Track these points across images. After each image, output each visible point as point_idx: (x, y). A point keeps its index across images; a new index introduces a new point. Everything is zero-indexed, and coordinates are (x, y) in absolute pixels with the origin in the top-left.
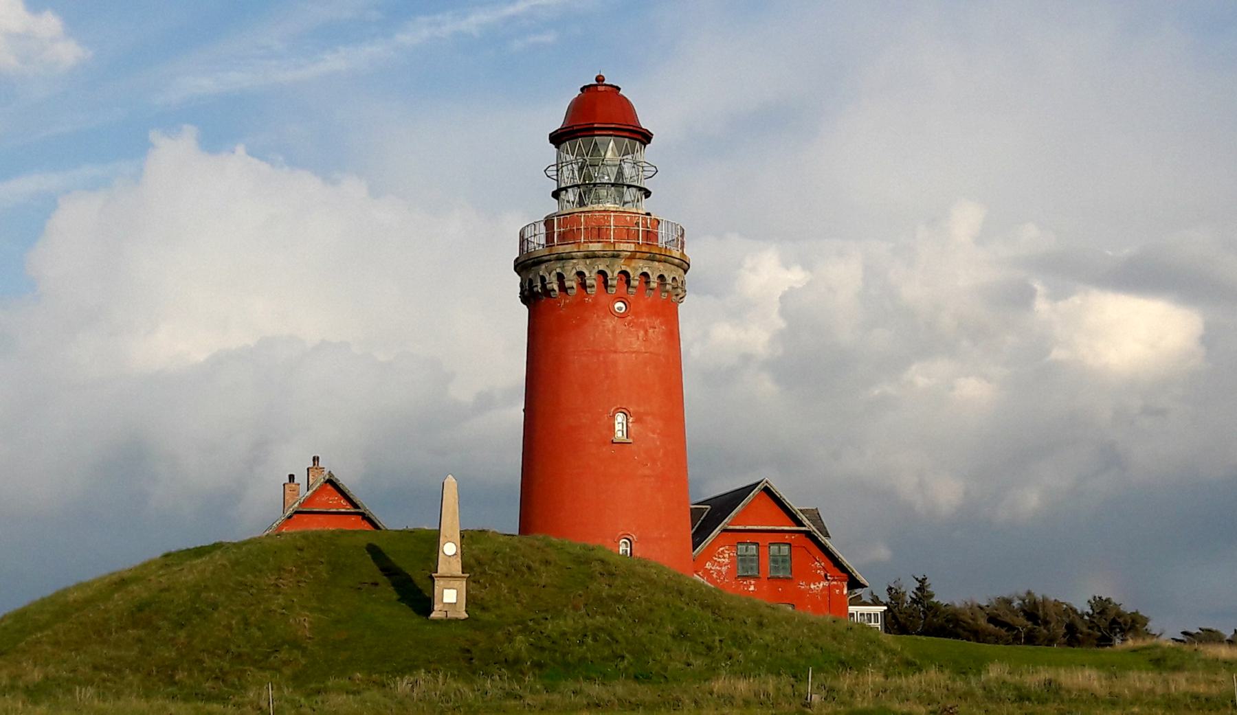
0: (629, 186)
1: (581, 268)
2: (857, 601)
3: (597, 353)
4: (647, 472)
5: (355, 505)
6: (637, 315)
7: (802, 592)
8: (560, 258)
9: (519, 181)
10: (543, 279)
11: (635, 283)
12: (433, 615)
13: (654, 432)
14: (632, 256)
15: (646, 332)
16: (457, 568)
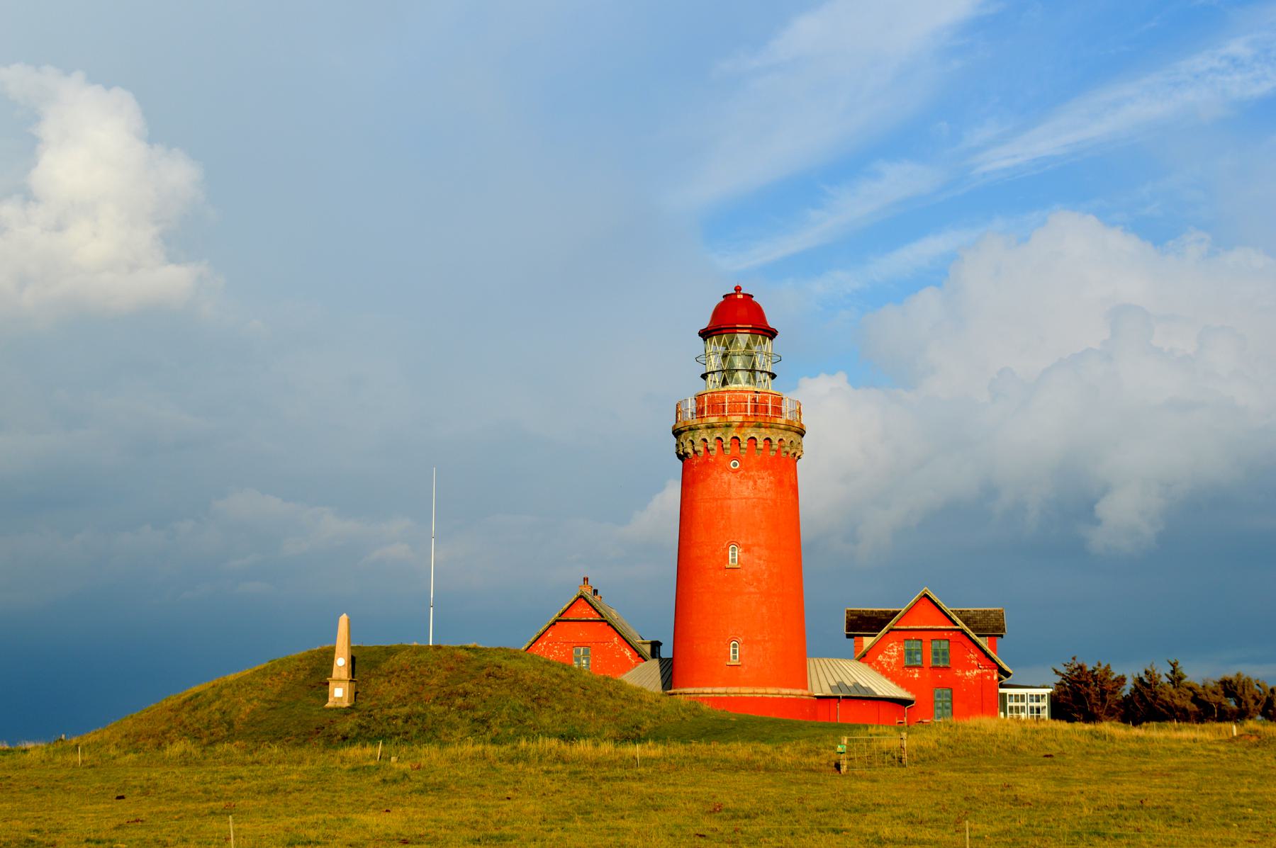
1: (704, 436)
2: (1002, 686)
3: (717, 500)
4: (753, 590)
5: (601, 615)
6: (747, 470)
7: (962, 678)
11: (744, 445)
12: (328, 705)
13: (760, 558)
14: (741, 426)
15: (755, 482)
16: (345, 674)
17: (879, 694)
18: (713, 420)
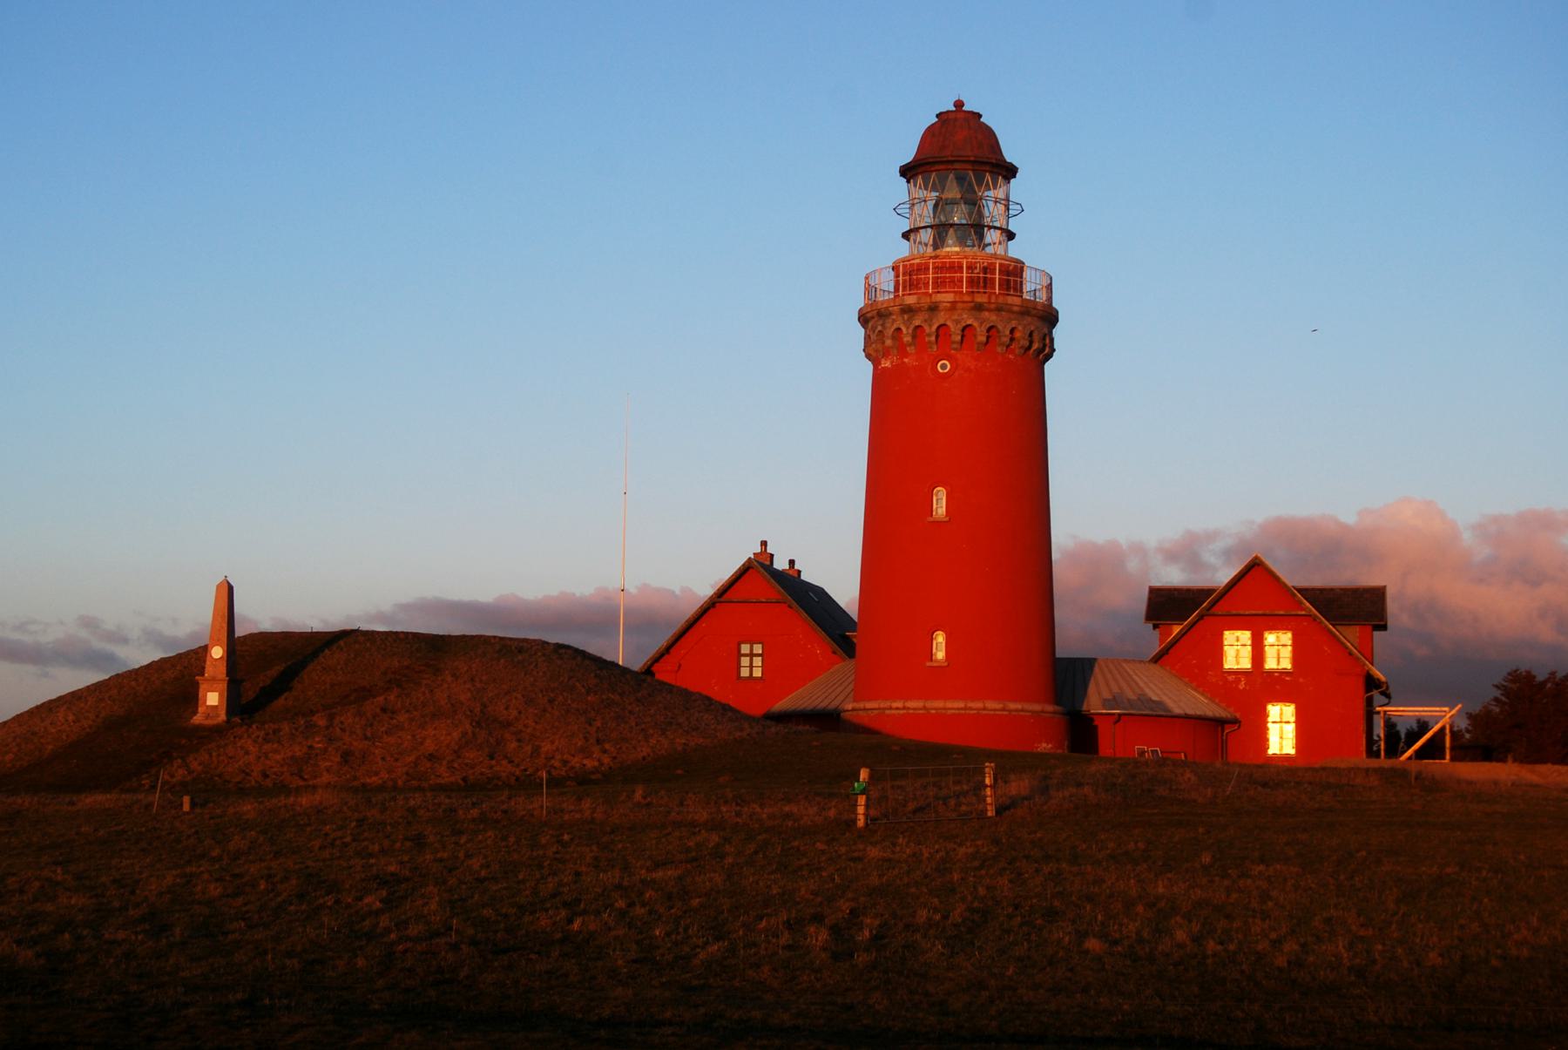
0: (990, 227)
1: (899, 323)
9: (876, 230)
17: (1177, 711)
18: (911, 300)
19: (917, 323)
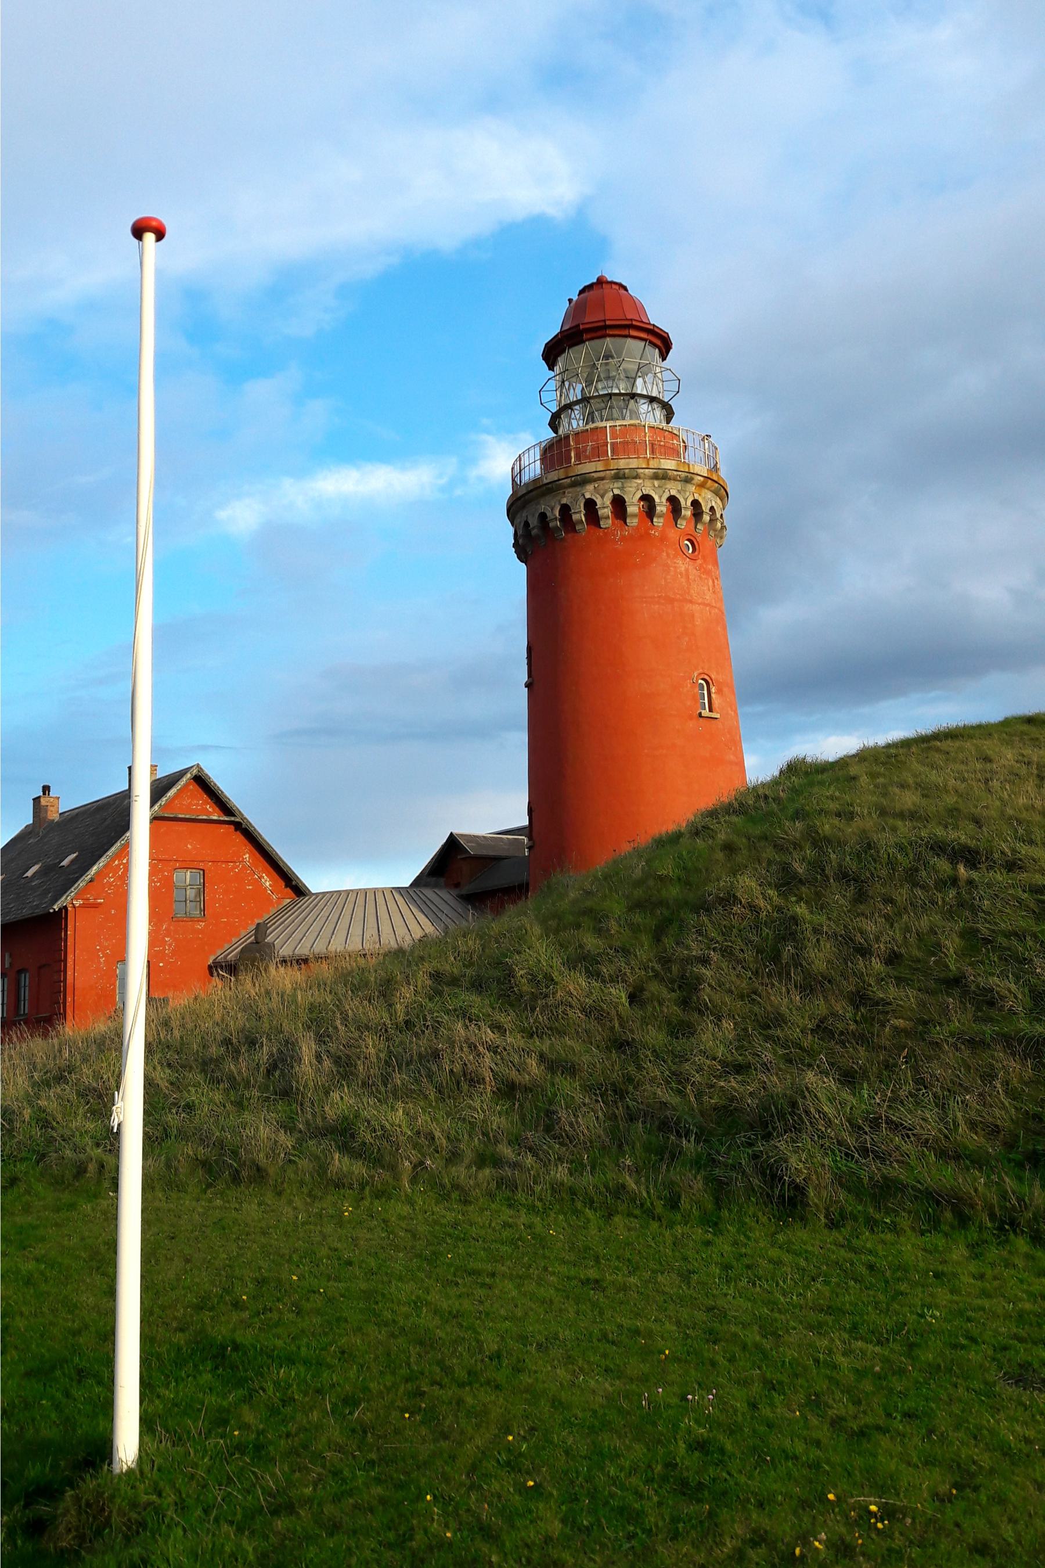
1: (648, 491)
3: (671, 601)
8: (619, 476)
10: (590, 505)
11: (706, 518)
18: (669, 464)
19: (673, 493)
